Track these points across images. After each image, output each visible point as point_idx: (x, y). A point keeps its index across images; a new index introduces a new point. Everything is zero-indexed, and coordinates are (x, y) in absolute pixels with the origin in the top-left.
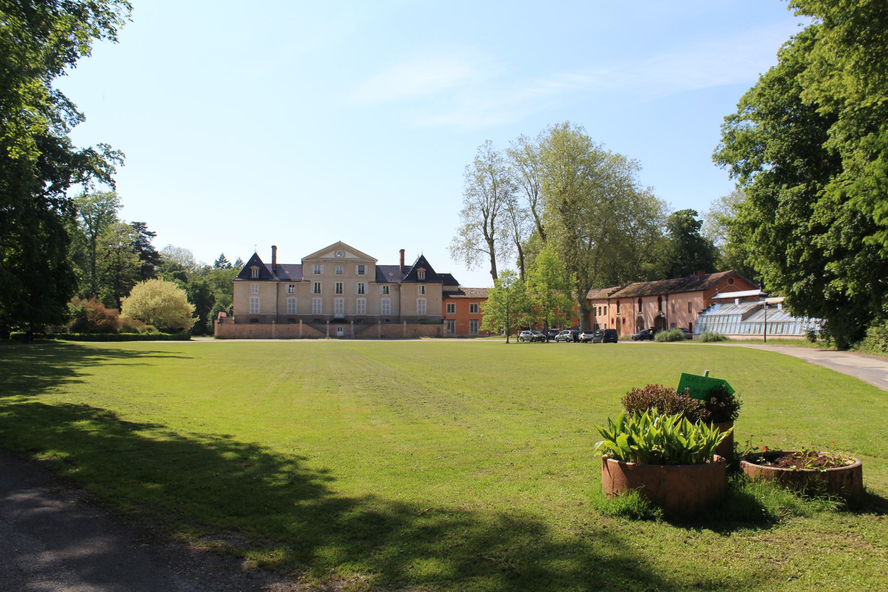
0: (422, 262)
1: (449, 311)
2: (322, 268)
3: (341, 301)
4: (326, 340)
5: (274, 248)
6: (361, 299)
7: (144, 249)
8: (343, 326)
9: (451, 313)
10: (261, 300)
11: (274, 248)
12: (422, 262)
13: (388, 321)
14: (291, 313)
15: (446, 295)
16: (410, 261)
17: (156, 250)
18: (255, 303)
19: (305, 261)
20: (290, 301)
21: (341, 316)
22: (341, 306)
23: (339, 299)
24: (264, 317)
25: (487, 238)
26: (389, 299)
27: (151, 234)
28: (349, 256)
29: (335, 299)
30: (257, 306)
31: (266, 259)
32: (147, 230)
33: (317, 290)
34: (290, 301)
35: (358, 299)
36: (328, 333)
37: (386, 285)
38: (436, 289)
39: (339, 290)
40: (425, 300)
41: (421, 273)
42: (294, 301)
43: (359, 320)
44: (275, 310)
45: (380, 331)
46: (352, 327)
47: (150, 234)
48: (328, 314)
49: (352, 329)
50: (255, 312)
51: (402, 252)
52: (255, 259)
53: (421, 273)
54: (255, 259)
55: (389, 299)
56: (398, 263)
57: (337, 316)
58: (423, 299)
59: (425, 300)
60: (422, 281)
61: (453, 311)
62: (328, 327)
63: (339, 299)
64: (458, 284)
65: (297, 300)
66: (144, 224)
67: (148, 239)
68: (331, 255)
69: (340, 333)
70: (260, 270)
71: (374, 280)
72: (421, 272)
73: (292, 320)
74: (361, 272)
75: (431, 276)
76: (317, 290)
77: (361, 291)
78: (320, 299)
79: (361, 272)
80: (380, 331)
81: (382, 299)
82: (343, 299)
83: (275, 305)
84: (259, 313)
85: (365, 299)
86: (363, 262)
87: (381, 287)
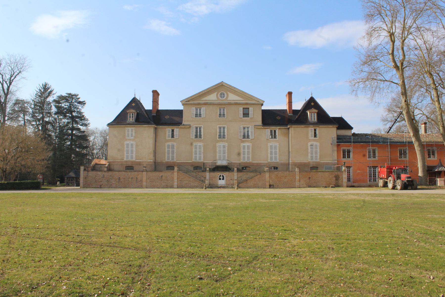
0: (311, 103)
1: (344, 157)
2: (203, 110)
3: (224, 147)
4: (203, 191)
5: (156, 94)
6: (246, 144)
7: (74, 114)
8: (225, 174)
9: (346, 160)
10: (137, 146)
11: (156, 94)
12: (311, 103)
13: (276, 168)
14: (170, 160)
15: (340, 139)
16: (298, 106)
17: (83, 114)
18: (130, 149)
19: (186, 102)
20: (169, 146)
21: (224, 163)
22: (224, 153)
23: (221, 145)
24: (139, 164)
25: (396, 67)
26: (277, 144)
27: (83, 103)
28: (232, 97)
29: (218, 144)
30: (132, 151)
31: (148, 105)
32: (80, 100)
33: (198, 135)
34: (169, 146)
35: (242, 144)
36: (207, 182)
37: (273, 128)
38: (330, 133)
39: (222, 136)
40: (318, 144)
41: (312, 115)
42: (173, 146)
43: (243, 168)
44: (152, 156)
45: (267, 179)
46: (235, 175)
47: (80, 103)
48: (209, 161)
49: (236, 178)
50: (130, 159)
51: (290, 94)
52: (135, 104)
53: (312, 115)
54: (135, 104)
55: (277, 144)
56: (285, 107)
57: (219, 163)
58: (315, 143)
59: (318, 144)
60: (313, 124)
61: (349, 157)
62: (207, 175)
63: (222, 144)
64: (351, 128)
65: (178, 146)
66: (76, 95)
67: (80, 108)
68: (213, 97)
69: (222, 182)
70: (138, 114)
71: (260, 123)
72: (311, 115)
73: (170, 167)
74: (246, 114)
75: (324, 118)
76: (198, 135)
77: (246, 136)
78: (201, 144)
79: (246, 114)
80: (267, 179)
81: (269, 144)
82: (226, 144)
83: (151, 150)
84: (134, 159)
85: (250, 144)
86: (247, 105)
87: (267, 131)
